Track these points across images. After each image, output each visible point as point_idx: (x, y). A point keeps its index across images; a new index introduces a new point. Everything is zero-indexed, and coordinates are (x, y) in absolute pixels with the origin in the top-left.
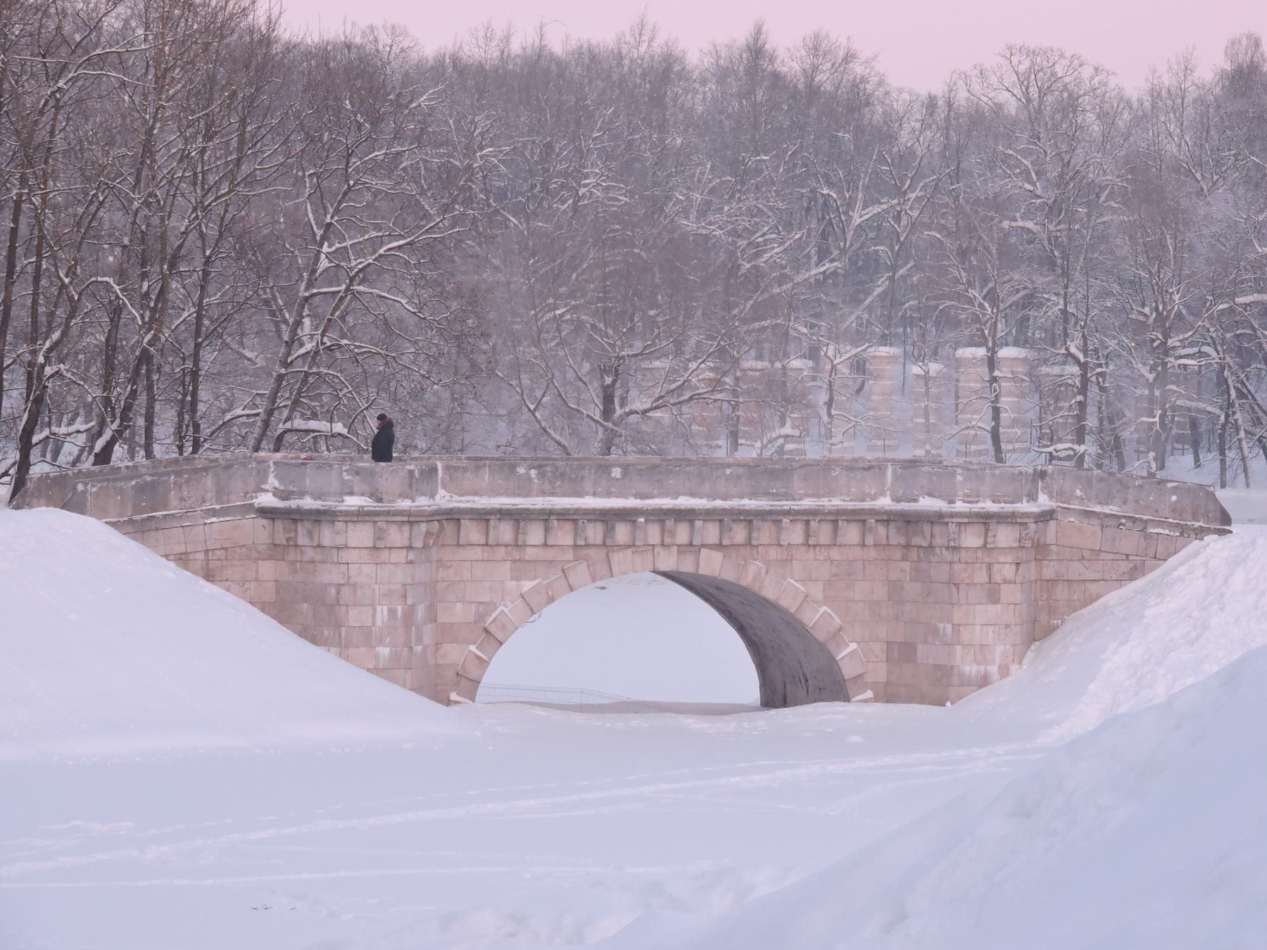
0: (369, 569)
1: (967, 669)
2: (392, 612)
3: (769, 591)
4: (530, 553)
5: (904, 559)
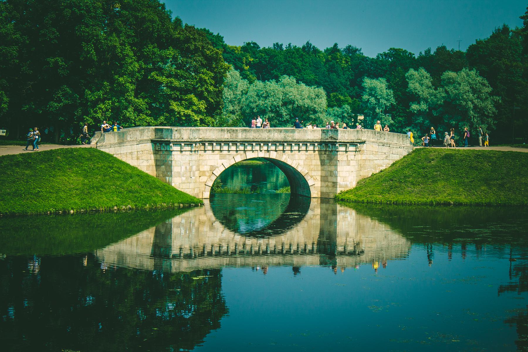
0: (180, 156)
1: (341, 183)
2: (186, 168)
3: (289, 162)
4: (224, 152)
5: (325, 154)
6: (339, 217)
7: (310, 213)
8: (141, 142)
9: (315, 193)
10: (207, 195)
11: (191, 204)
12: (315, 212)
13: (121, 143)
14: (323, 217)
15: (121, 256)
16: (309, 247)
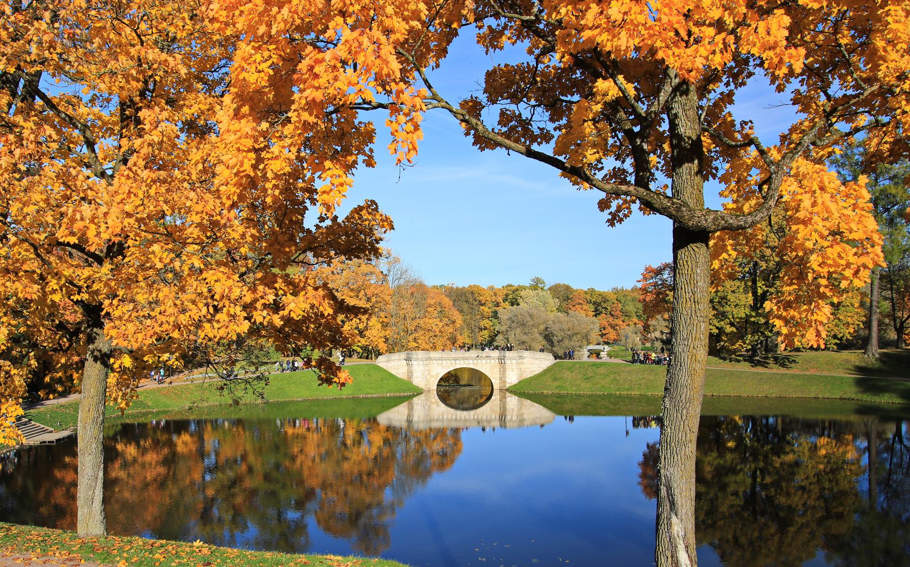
6: (508, 399)
7: (493, 397)
9: (496, 387)
12: (496, 397)
13: (388, 361)
14: (501, 400)
15: (389, 419)
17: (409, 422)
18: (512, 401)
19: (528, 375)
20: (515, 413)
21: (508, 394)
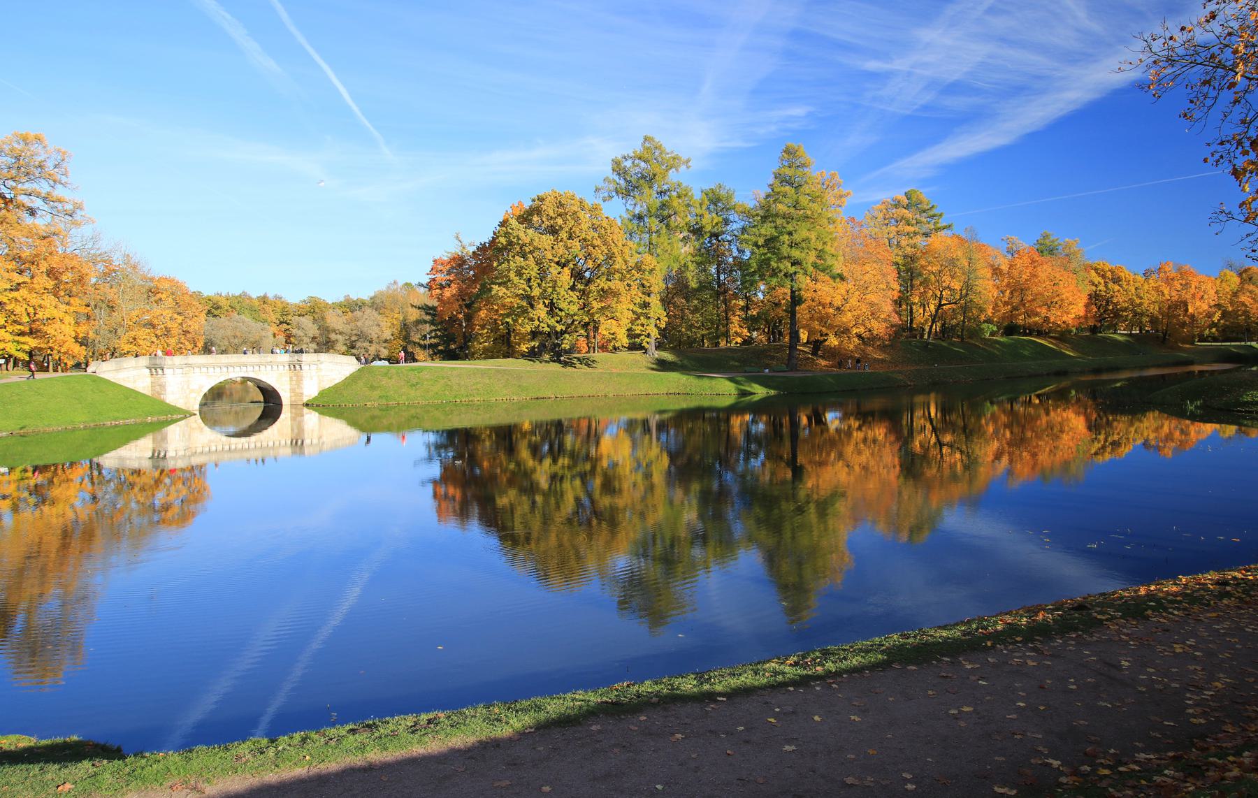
8: (136, 368)
10: (197, 407)
11: (187, 414)
14: (293, 419)
16: (283, 443)
17: (157, 457)
18: (312, 419)
19: (327, 384)
20: (316, 434)
21: (306, 410)
